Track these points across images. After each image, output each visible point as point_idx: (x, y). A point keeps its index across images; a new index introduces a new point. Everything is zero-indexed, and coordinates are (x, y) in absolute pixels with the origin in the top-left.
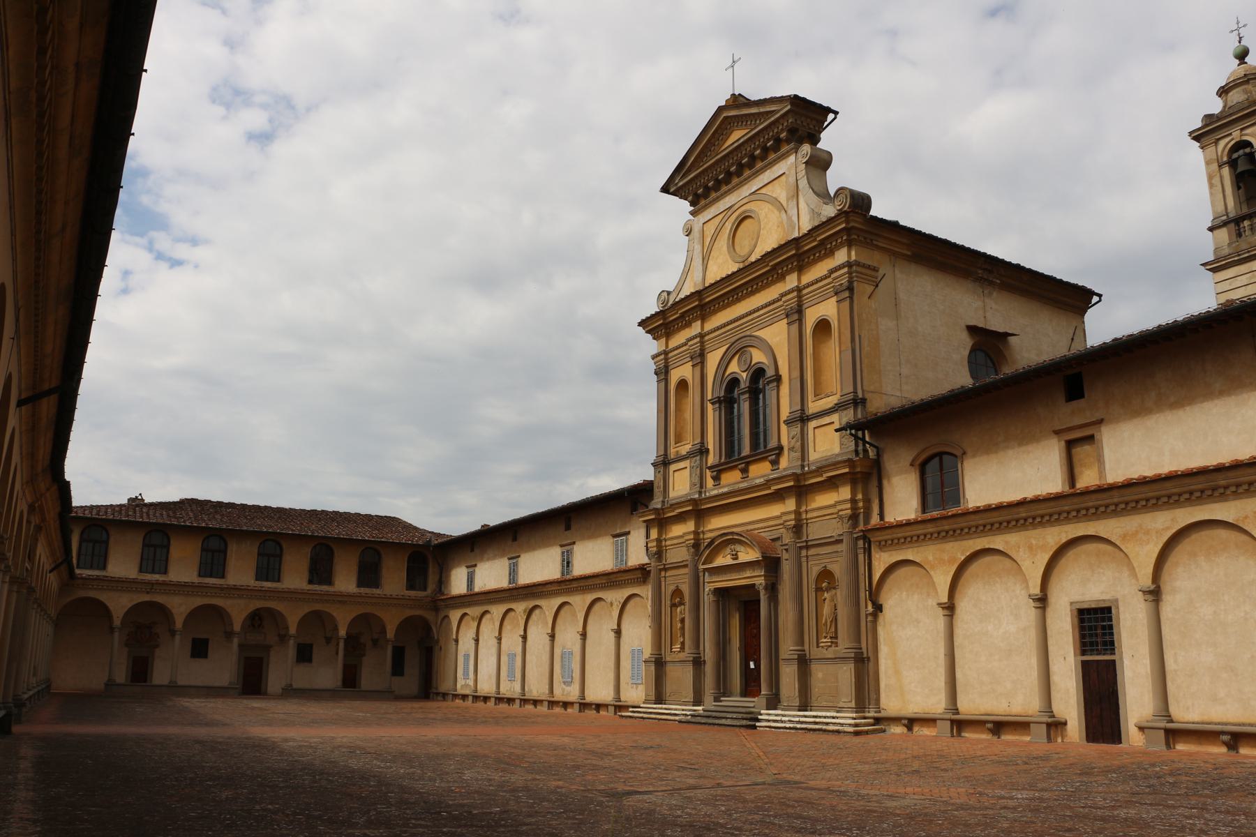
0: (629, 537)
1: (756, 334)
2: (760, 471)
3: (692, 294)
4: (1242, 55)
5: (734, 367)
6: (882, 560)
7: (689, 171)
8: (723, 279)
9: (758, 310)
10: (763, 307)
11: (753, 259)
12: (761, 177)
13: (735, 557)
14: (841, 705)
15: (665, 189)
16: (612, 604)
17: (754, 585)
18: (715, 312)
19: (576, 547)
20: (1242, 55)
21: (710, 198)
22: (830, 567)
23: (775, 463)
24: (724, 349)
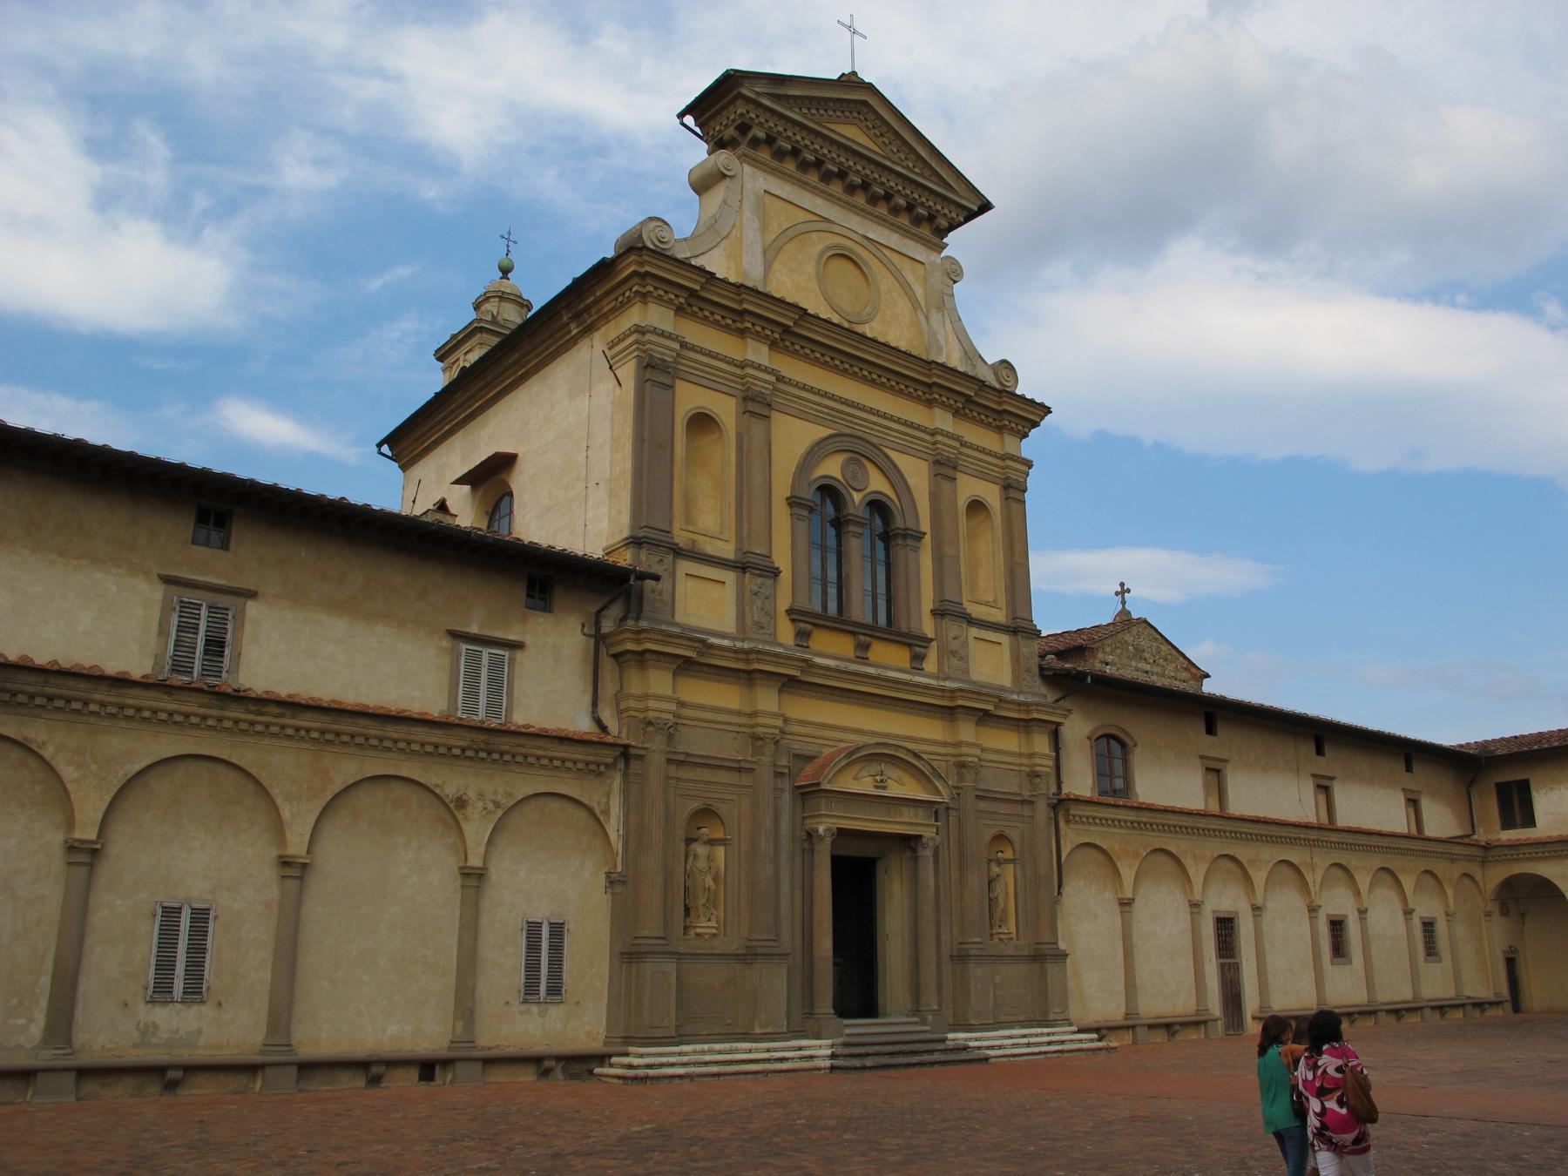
0: (519, 655)
1: (893, 455)
2: (889, 659)
3: (795, 307)
4: (505, 271)
5: (832, 468)
6: (1071, 837)
7: (777, 98)
8: (1032, 401)
9: (811, 390)
10: (899, 421)
11: (859, 329)
12: (886, 232)
13: (881, 785)
14: (1052, 1017)
15: (986, 206)
16: (461, 803)
17: (920, 837)
18: (795, 354)
19: (252, 609)
20: (505, 271)
21: (804, 178)
22: (1008, 832)
23: (918, 659)
24: (829, 432)
